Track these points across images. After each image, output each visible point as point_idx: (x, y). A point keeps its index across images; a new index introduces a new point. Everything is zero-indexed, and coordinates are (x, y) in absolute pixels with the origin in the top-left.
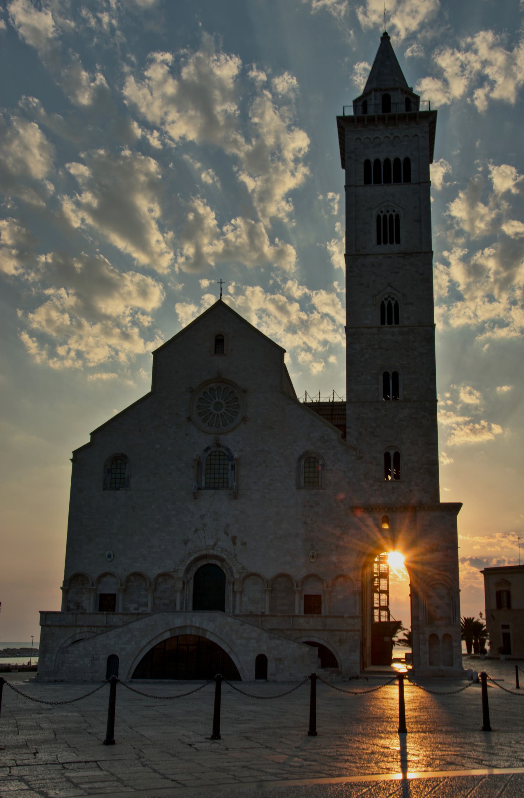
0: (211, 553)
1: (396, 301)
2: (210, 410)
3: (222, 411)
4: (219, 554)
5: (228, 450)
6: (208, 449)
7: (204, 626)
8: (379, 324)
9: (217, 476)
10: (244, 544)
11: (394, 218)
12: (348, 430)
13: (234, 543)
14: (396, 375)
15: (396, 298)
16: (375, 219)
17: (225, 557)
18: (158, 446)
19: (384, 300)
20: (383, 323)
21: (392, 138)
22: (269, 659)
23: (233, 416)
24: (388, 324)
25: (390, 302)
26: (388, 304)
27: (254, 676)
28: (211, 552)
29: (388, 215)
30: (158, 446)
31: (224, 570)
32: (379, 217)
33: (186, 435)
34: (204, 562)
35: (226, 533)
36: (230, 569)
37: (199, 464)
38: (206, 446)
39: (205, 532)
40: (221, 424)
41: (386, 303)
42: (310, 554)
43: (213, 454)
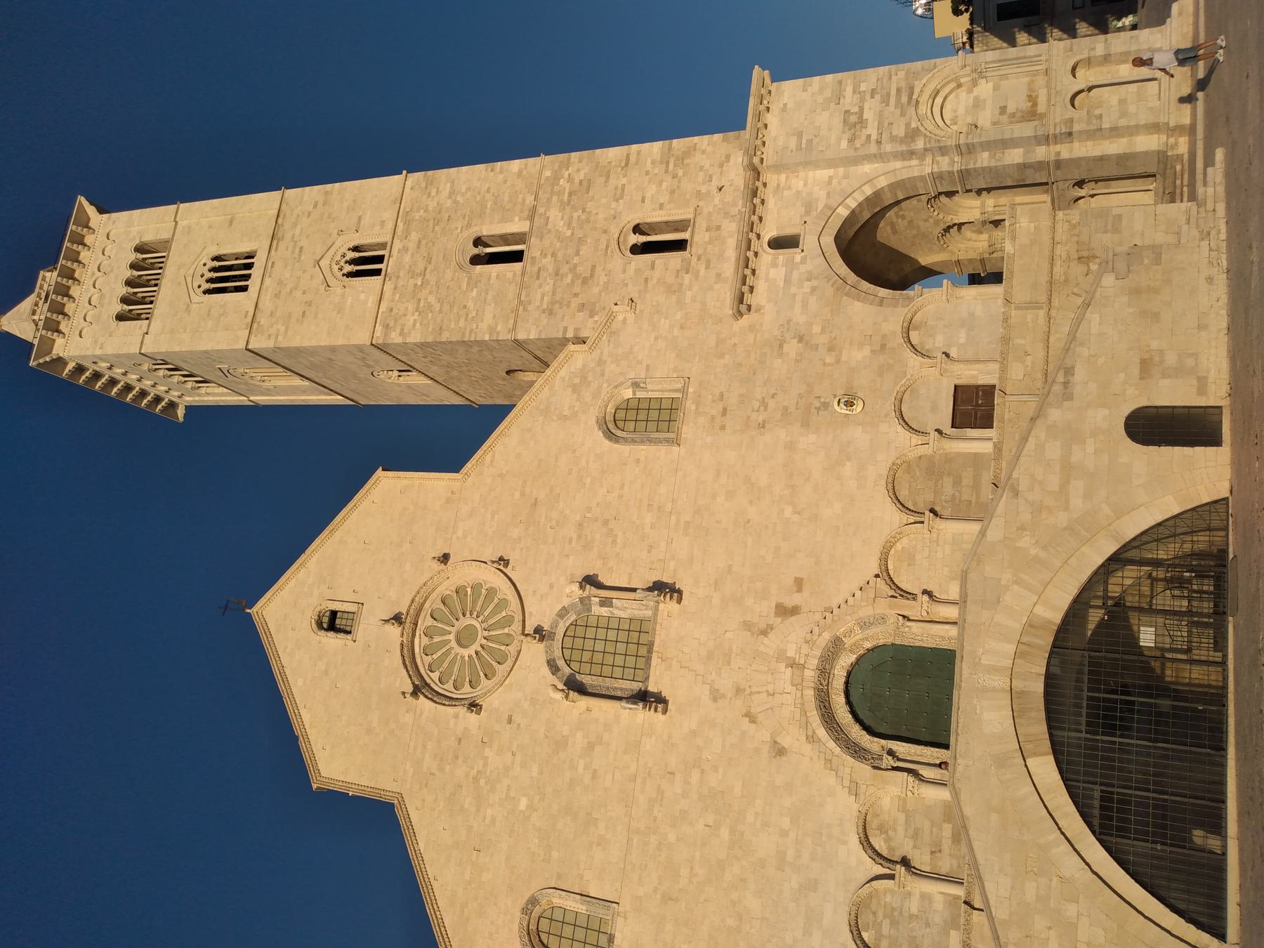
0: (812, 673)
1: (349, 250)
2: (470, 657)
3: (478, 626)
4: (818, 653)
5: (563, 613)
7: (1015, 625)
9: (621, 648)
10: (799, 584)
12: (570, 335)
13: (795, 611)
14: (478, 242)
15: (344, 250)
17: (827, 636)
18: (523, 804)
19: (342, 272)
20: (377, 272)
22: (1143, 402)
23: (496, 601)
24: (382, 262)
25: (346, 262)
26: (350, 265)
27: (1211, 450)
28: (810, 674)
30: (523, 804)
31: (868, 645)
33: (510, 721)
34: (839, 701)
35: (764, 633)
36: (864, 625)
37: (582, 690)
38: (546, 670)
39: (759, 692)
40: (506, 631)
41: (349, 268)
42: (842, 410)
43: (567, 653)
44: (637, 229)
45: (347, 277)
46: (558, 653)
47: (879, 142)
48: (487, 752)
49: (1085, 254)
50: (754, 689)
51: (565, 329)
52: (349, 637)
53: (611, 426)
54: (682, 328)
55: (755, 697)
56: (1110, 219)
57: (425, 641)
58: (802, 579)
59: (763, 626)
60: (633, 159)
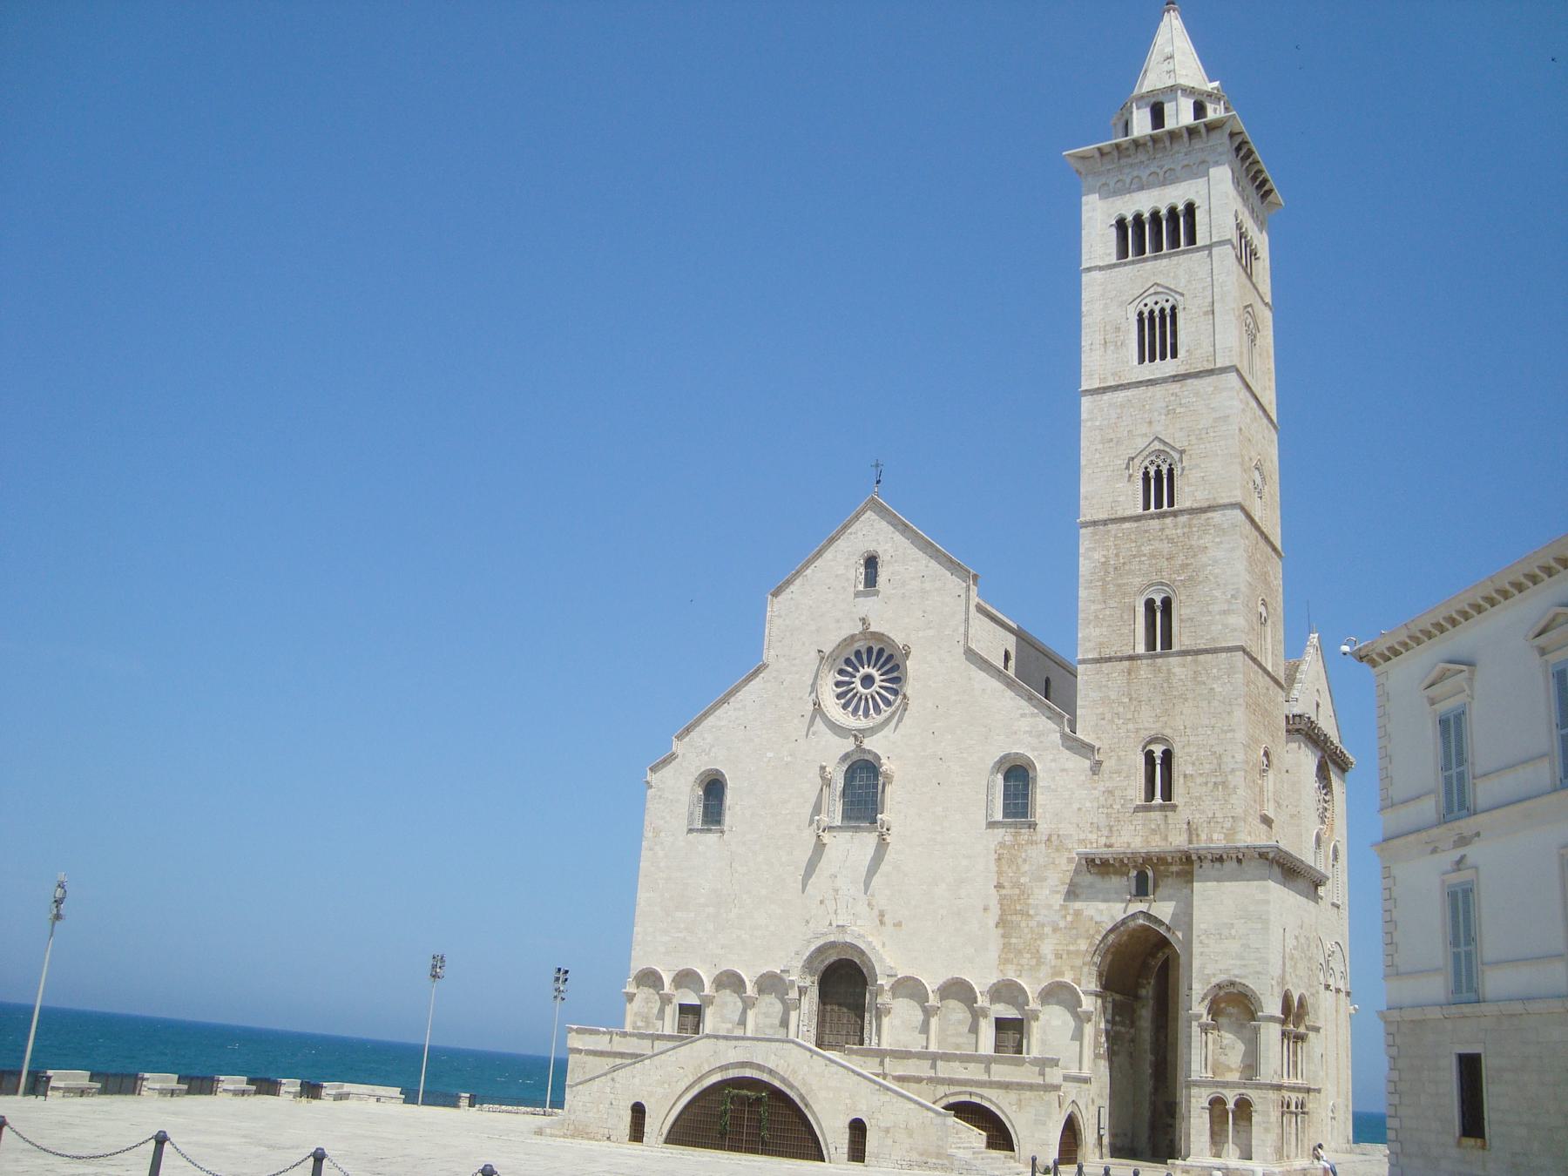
6: (846, 757)
8: (1140, 511)
11: (1168, 311)
12: (1079, 712)
13: (882, 923)
16: (1134, 319)
17: (863, 946)
21: (1161, 174)
26: (1156, 472)
29: (1157, 310)
32: (1141, 314)
35: (869, 905)
44: (1168, 756)
45: (1144, 474)
46: (855, 758)
47: (1202, 954)
48: (796, 721)
49: (1023, 1103)
50: (838, 901)
51: (1083, 707)
52: (861, 587)
53: (1007, 765)
54: (1079, 809)
55: (834, 902)
56: (1044, 1119)
57: (864, 650)
58: (901, 926)
59: (874, 903)
60: (1229, 735)
